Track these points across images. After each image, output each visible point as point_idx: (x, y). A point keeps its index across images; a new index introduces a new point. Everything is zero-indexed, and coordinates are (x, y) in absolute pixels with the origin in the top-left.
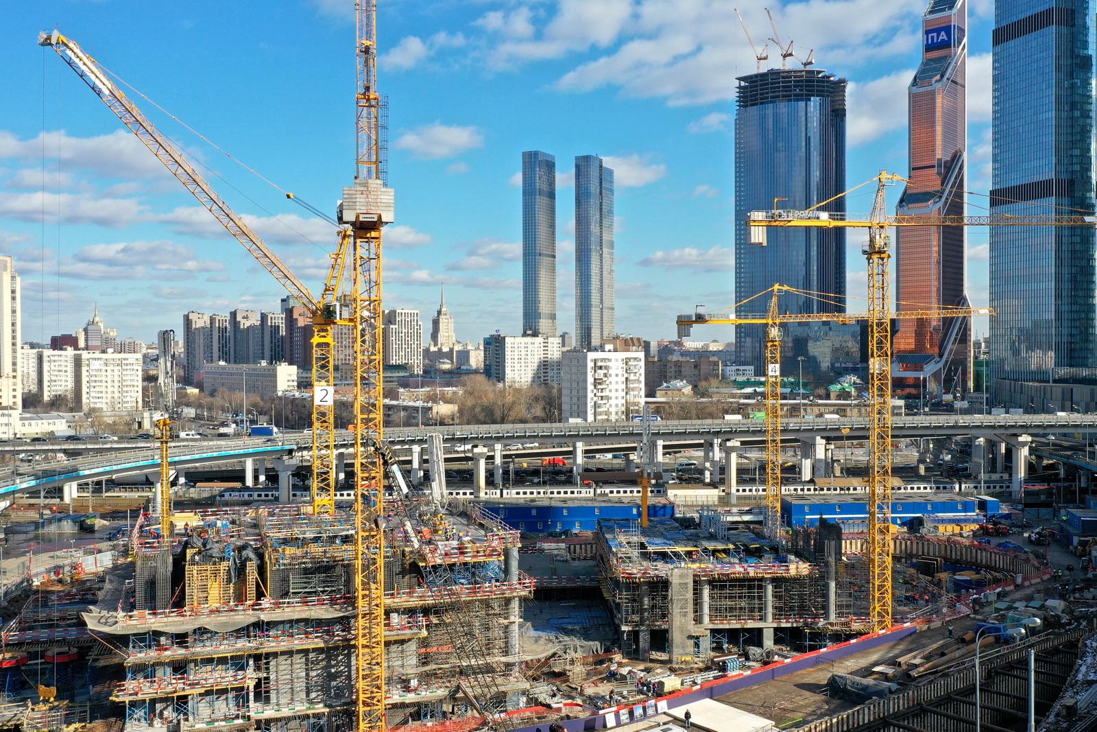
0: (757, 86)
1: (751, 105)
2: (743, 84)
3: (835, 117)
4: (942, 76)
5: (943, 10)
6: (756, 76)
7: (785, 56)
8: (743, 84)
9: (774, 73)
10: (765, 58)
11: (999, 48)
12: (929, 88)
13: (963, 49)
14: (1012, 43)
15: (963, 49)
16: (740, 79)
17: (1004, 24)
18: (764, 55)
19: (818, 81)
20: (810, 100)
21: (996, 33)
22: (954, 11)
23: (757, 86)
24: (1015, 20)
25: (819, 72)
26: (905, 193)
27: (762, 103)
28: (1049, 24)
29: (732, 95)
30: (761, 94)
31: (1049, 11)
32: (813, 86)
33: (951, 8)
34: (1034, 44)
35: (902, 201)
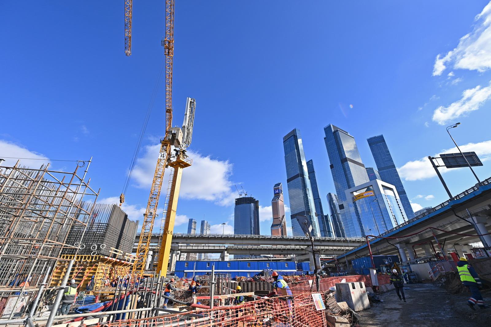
3: (257, 208)
4: (278, 199)
6: (239, 198)
7: (245, 195)
9: (243, 198)
11: (288, 183)
14: (291, 182)
16: (236, 199)
17: (289, 178)
21: (287, 180)
26: (272, 224)
28: (299, 177)
29: (234, 202)
31: (298, 174)
33: (279, 186)
35: (272, 226)
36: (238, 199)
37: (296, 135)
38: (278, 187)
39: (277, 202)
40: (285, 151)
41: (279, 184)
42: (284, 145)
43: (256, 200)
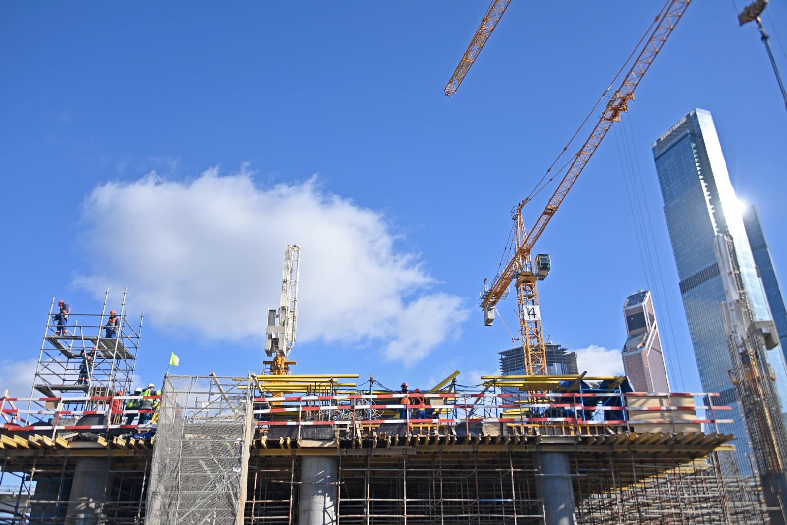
0: (514, 357)
1: (511, 370)
2: (504, 357)
5: (637, 303)
6: (513, 350)
8: (504, 357)
10: (518, 339)
11: (686, 294)
12: (636, 352)
13: (655, 328)
15: (655, 328)
16: (502, 354)
17: (686, 278)
18: (517, 338)
19: (556, 353)
20: (552, 365)
22: (644, 303)
23: (514, 357)
24: (694, 274)
25: (557, 347)
27: (518, 369)
30: (517, 363)
32: (553, 356)
33: (642, 300)
34: (713, 287)
36: (509, 352)
37: (696, 132)
38: (639, 304)
39: (640, 354)
40: (662, 190)
41: (641, 297)
42: (657, 168)
43: (568, 352)
